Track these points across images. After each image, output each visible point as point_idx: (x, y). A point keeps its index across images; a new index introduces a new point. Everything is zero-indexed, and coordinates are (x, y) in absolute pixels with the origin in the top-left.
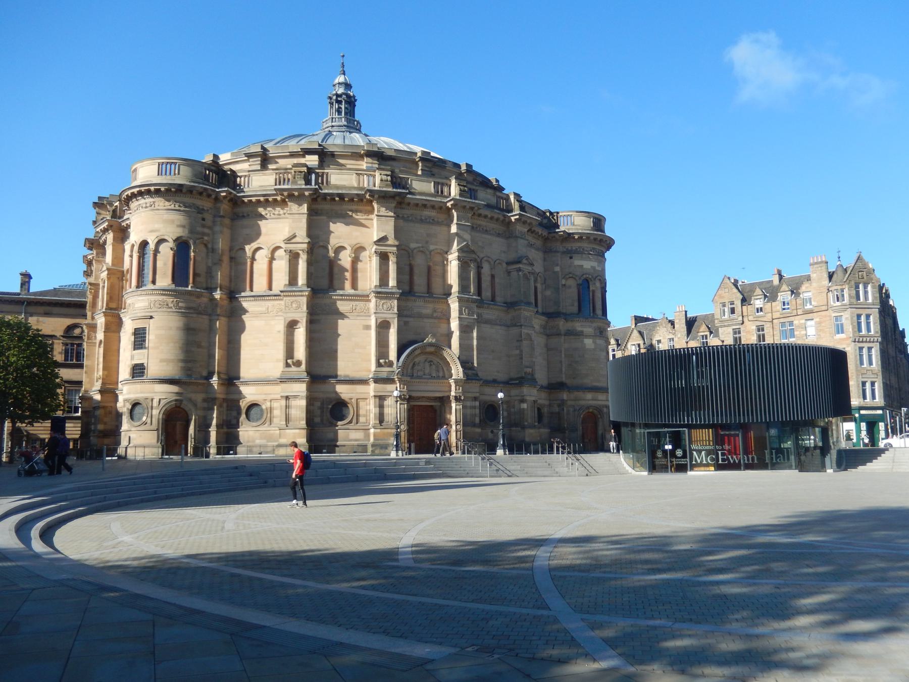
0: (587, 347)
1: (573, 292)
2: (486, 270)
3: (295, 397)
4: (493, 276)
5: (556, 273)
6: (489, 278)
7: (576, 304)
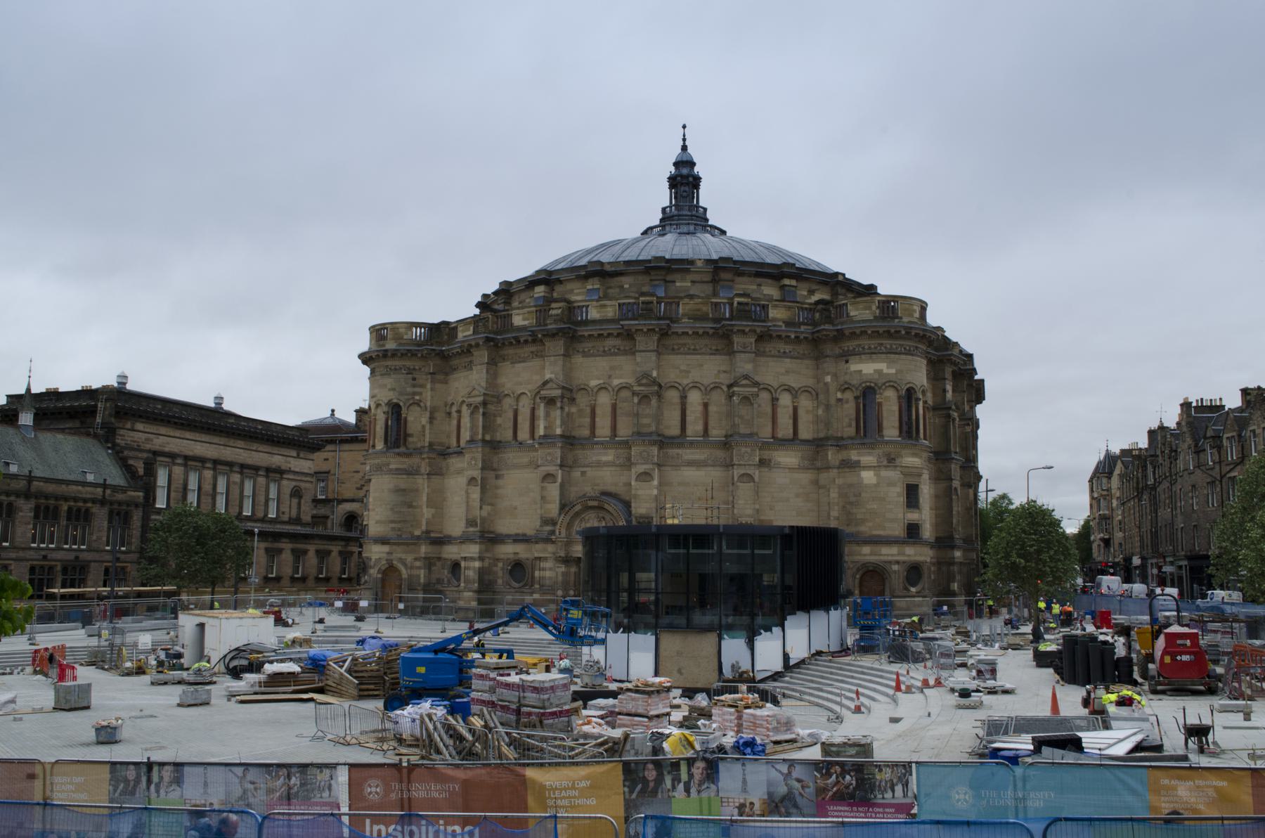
0: (866, 482)
1: (850, 408)
2: (695, 398)
3: (472, 559)
4: (706, 405)
5: (826, 384)
6: (700, 408)
7: (854, 424)
